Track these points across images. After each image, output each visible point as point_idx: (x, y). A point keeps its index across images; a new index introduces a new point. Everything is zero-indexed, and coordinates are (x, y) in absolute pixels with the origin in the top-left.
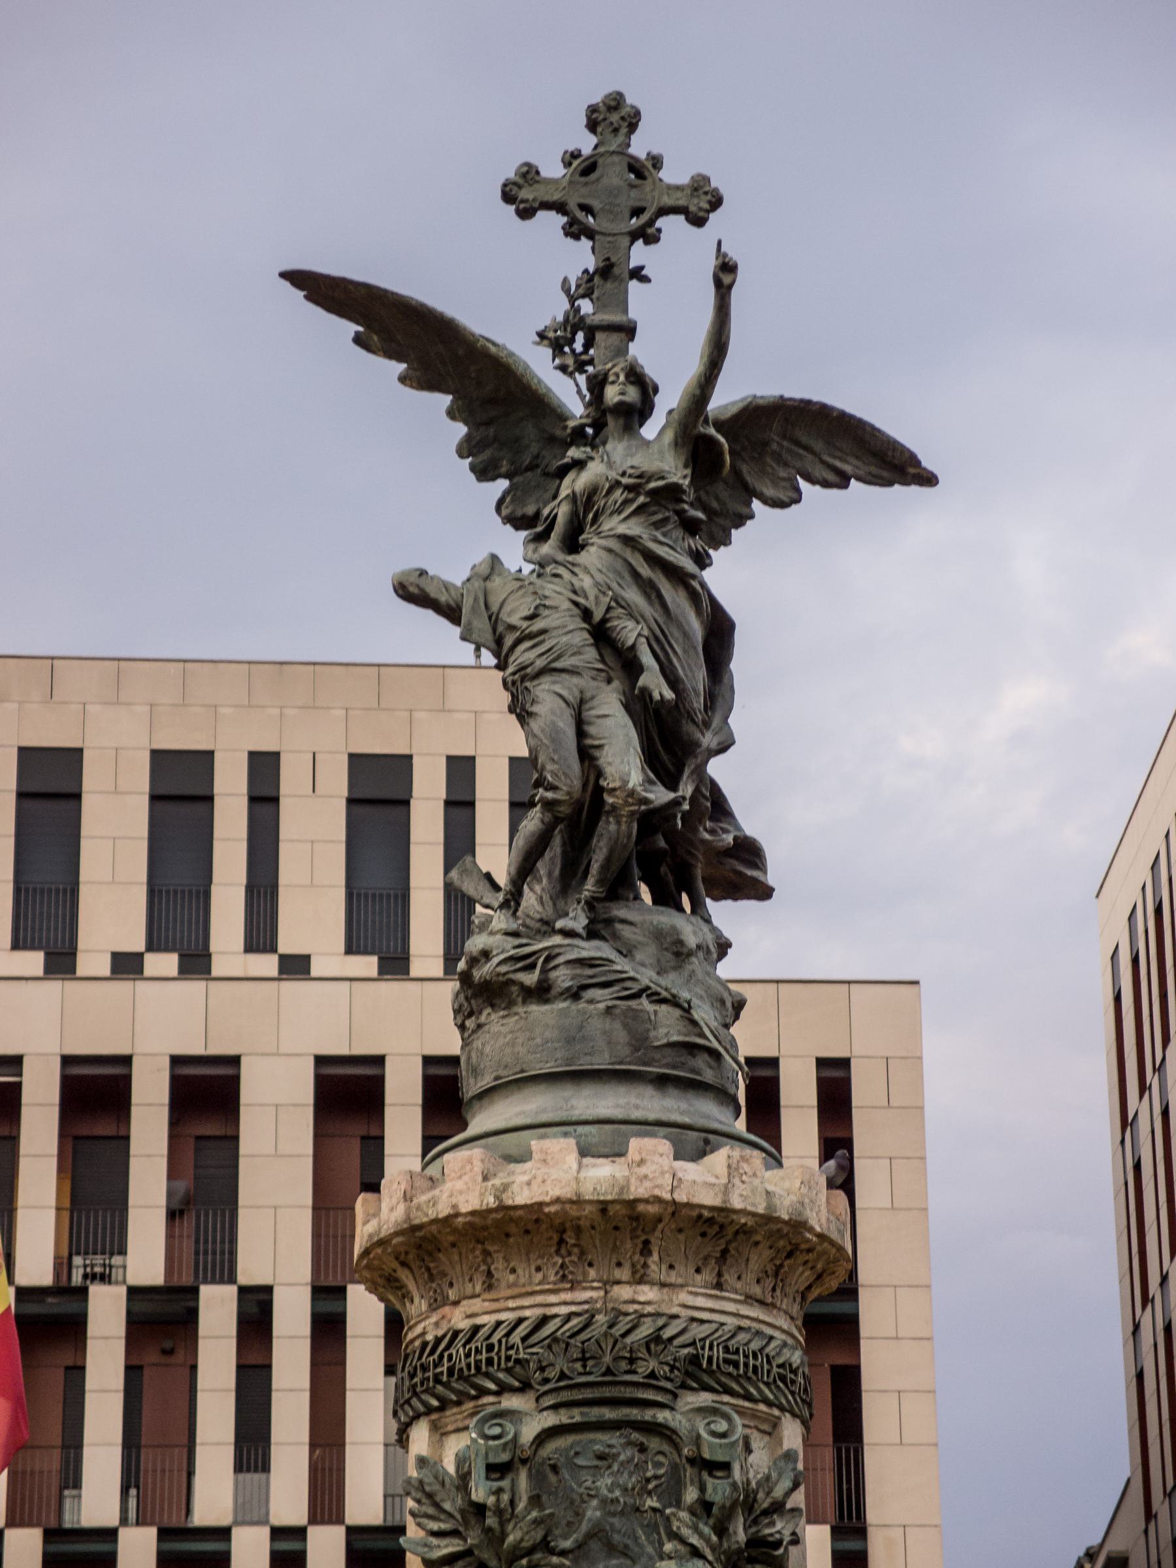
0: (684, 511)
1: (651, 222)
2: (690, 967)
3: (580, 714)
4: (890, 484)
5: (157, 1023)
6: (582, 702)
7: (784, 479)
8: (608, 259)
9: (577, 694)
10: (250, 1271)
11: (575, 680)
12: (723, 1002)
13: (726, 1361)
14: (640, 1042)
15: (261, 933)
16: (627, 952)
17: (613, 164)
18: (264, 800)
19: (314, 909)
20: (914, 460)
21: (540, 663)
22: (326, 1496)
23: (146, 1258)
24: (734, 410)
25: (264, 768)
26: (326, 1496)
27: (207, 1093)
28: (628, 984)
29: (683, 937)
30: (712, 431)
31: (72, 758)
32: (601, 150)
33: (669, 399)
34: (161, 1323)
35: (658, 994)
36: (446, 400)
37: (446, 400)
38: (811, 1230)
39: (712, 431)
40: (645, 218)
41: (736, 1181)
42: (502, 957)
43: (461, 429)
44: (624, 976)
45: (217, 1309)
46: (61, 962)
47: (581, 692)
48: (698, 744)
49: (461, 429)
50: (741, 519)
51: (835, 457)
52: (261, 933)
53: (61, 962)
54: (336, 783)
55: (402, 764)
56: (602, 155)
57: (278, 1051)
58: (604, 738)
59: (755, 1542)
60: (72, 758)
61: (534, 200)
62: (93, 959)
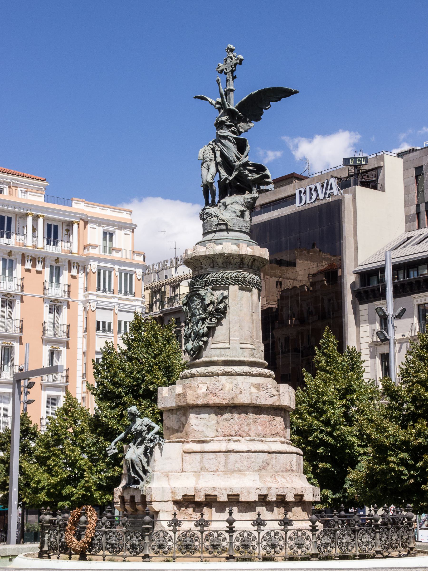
4: (290, 96)
13: (213, 280)
38: (226, 254)
41: (208, 249)
50: (262, 113)
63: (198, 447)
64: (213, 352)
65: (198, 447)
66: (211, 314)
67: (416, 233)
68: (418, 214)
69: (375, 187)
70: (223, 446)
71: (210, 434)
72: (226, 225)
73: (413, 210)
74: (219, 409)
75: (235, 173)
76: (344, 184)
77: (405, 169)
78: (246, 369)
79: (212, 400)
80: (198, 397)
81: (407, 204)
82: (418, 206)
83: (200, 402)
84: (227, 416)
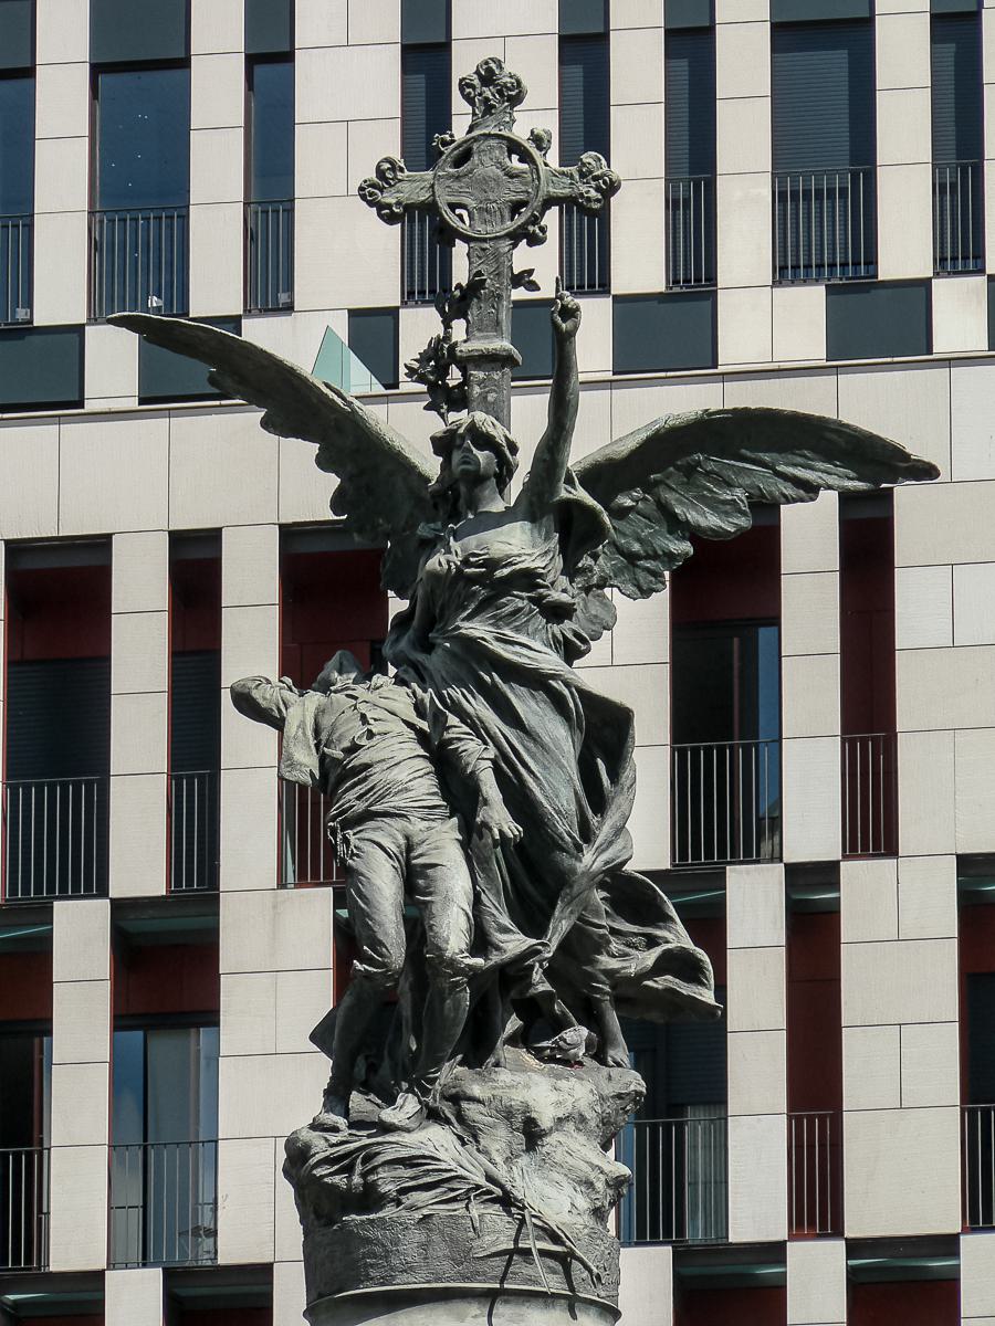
0: (543, 597)
1: (535, 220)
2: (544, 1150)
3: (408, 860)
6: (410, 848)
7: (725, 502)
8: (479, 273)
9: (402, 841)
11: (398, 823)
12: (590, 1184)
14: (462, 1255)
16: (470, 1134)
17: (492, 148)
20: (898, 454)
21: (360, 806)
24: (632, 444)
28: (455, 1185)
29: (534, 1115)
30: (581, 494)
32: (476, 133)
33: (524, 463)
35: (489, 1192)
36: (314, 448)
37: (314, 448)
39: (581, 494)
40: (526, 213)
42: (318, 1157)
43: (334, 481)
44: (453, 1174)
47: (407, 838)
48: (573, 871)
49: (334, 481)
51: (795, 465)
56: (475, 139)
58: (430, 894)
61: (398, 203)
72: (565, 1260)
75: (560, 926)
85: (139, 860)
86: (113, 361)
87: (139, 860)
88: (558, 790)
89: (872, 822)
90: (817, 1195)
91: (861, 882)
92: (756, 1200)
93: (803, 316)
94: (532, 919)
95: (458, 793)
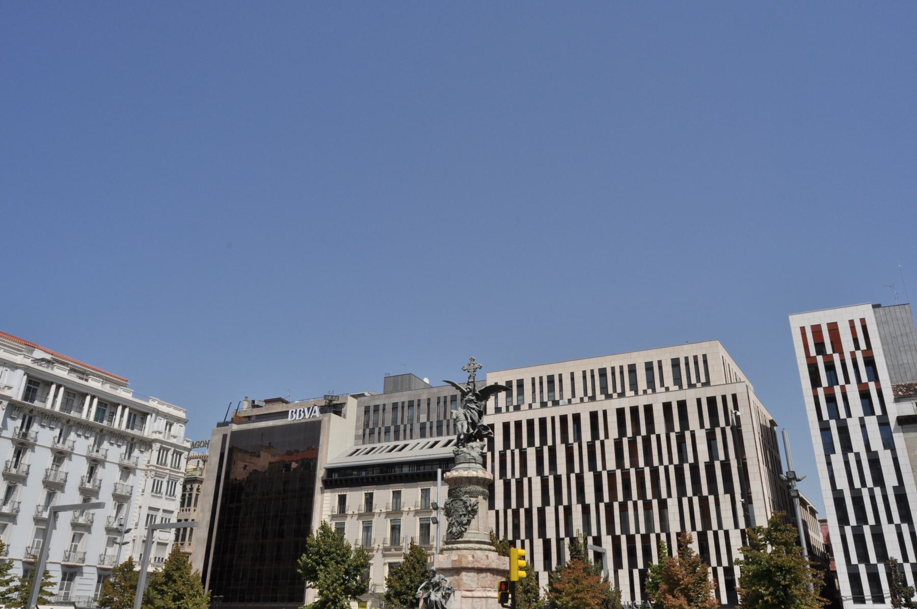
5: (641, 402)
10: (657, 432)
15: (662, 385)
18: (660, 367)
19: (669, 380)
22: (671, 461)
23: (644, 432)
25: (660, 362)
26: (671, 461)
27: (649, 409)
31: (634, 365)
34: (647, 441)
45: (653, 438)
46: (636, 393)
52: (662, 385)
53: (636, 393)
54: (670, 363)
55: (678, 359)
57: (657, 402)
59: (472, 510)
60: (634, 365)
62: (640, 392)
63: (469, 594)
64: (470, 535)
65: (469, 594)
66: (469, 512)
67: (363, 447)
68: (364, 435)
69: (340, 415)
70: (484, 594)
71: (474, 586)
73: (361, 432)
74: (480, 570)
76: (323, 410)
77: (358, 406)
78: (478, 546)
79: (477, 565)
80: (469, 563)
81: (357, 428)
82: (364, 430)
83: (470, 566)
84: (484, 575)
85: (550, 443)
86: (550, 404)
87: (550, 443)
88: (476, 418)
89: (607, 437)
90: (604, 467)
91: (606, 441)
92: (599, 468)
93: (603, 397)
94: (474, 429)
95: (467, 419)
